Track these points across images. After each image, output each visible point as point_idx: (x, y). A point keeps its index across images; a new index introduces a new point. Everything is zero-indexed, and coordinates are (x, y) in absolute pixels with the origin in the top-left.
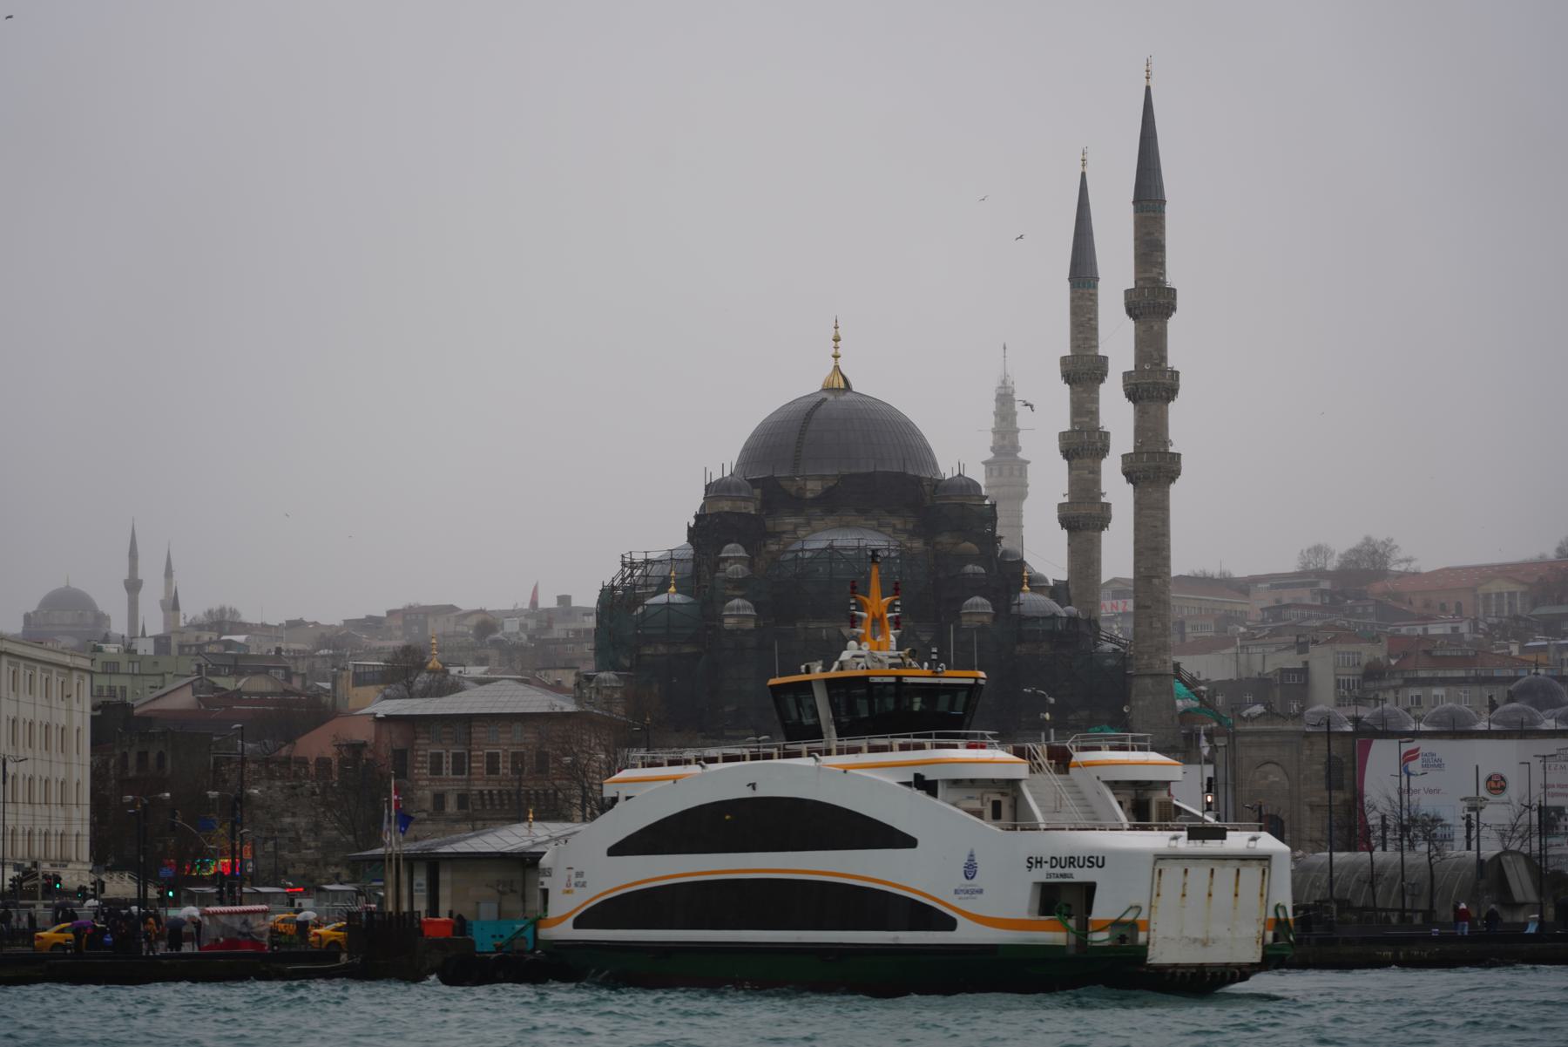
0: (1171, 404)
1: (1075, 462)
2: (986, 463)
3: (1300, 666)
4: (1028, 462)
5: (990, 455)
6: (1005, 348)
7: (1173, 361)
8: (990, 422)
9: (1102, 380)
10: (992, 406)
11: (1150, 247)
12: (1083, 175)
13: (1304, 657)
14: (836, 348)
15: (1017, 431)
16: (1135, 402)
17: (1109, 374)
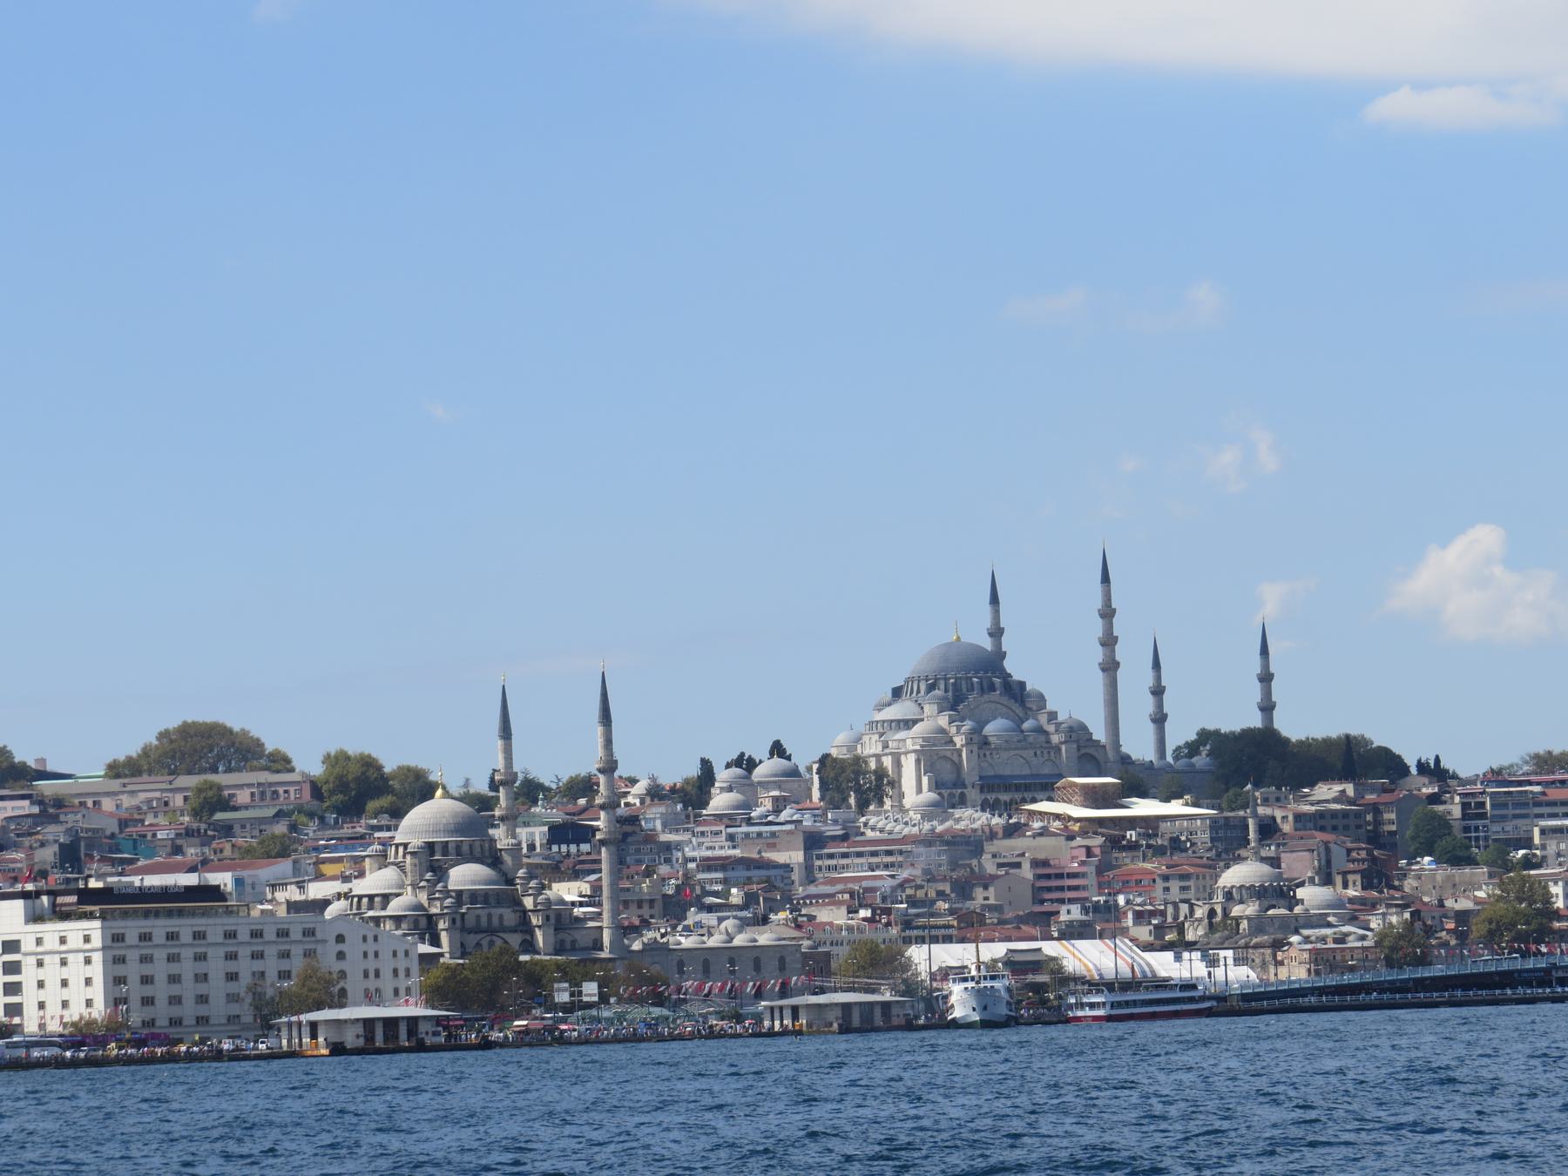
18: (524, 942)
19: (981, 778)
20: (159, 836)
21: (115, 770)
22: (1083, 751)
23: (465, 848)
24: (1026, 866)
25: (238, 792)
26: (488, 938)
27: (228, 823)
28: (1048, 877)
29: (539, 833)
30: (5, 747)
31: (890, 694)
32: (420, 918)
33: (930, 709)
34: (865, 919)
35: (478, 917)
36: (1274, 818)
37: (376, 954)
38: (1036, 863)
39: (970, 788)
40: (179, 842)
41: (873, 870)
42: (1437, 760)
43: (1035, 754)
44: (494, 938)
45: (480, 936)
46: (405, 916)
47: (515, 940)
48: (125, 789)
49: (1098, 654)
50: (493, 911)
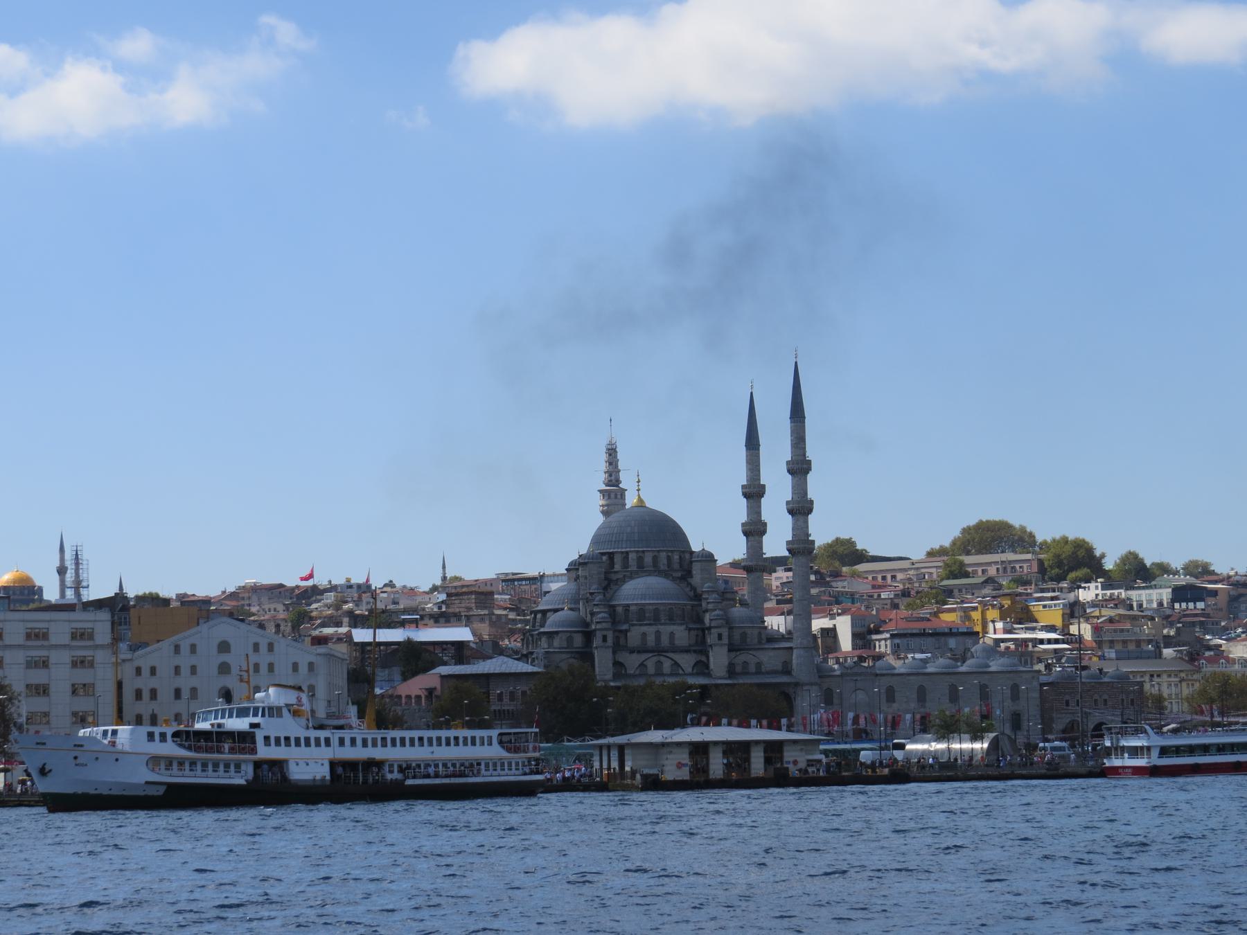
1: (751, 538)
3: (831, 626)
4: (626, 490)
5: (604, 487)
6: (611, 420)
7: (810, 495)
8: (603, 466)
9: (763, 497)
10: (604, 457)
11: (799, 440)
12: (752, 393)
13: (833, 622)
14: (638, 486)
15: (619, 471)
16: (793, 516)
17: (766, 493)
20: (882, 597)
21: (931, 554)
23: (648, 559)
25: (989, 568)
26: (655, 659)
27: (951, 588)
29: (1166, 594)
30: (851, 538)
32: (575, 635)
35: (644, 634)
37: (271, 667)
40: (896, 601)
44: (662, 659)
45: (643, 657)
46: (557, 633)
47: (687, 661)
48: (914, 566)
50: (661, 628)
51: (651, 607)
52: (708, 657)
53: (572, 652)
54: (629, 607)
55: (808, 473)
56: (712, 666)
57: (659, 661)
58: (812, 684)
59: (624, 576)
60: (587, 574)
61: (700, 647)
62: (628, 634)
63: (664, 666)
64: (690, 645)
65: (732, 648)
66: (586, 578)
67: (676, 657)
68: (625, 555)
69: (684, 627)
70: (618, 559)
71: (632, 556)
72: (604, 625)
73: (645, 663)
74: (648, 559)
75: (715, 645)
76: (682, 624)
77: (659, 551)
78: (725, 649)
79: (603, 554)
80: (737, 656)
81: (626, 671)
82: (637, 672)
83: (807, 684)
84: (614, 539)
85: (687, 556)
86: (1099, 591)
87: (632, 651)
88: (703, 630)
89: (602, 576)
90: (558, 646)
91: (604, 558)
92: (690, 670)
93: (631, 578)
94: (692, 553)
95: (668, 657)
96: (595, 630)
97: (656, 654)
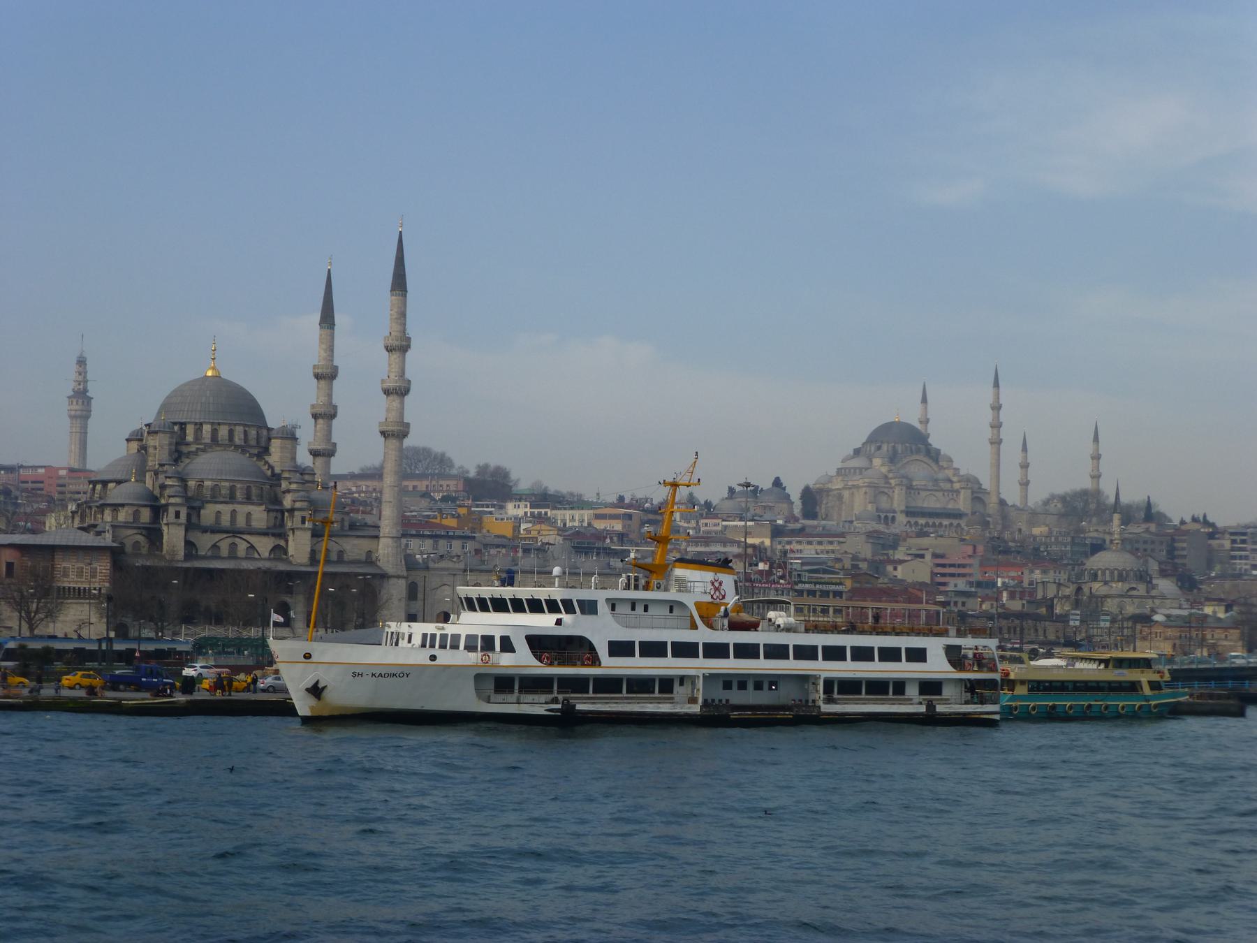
0: (406, 397)
2: (69, 397)
4: (92, 398)
8: (73, 375)
10: (75, 367)
18: (276, 548)
19: (907, 507)
22: (975, 495)
23: (223, 432)
24: (928, 557)
26: (230, 540)
28: (943, 566)
31: (852, 453)
33: (877, 462)
34: (761, 572)
36: (1104, 541)
38: (935, 556)
39: (899, 514)
41: (818, 554)
42: (1205, 516)
43: (944, 494)
44: (237, 539)
45: (218, 537)
46: (123, 505)
47: (264, 545)
49: (989, 433)
50: (238, 507)
51: (227, 484)
52: (287, 541)
53: (139, 528)
54: (203, 482)
55: (407, 351)
56: (291, 551)
57: (233, 543)
58: (398, 577)
59: (197, 449)
60: (157, 444)
61: (278, 531)
62: (202, 512)
63: (239, 548)
64: (268, 528)
65: (316, 534)
66: (155, 448)
67: (252, 539)
68: (198, 426)
69: (263, 507)
70: (190, 430)
71: (207, 428)
72: (177, 500)
73: (217, 544)
74: (223, 432)
75: (298, 529)
76: (261, 504)
77: (235, 425)
78: (309, 534)
79: (175, 424)
80: (318, 542)
81: (197, 552)
82: (209, 554)
83: (394, 577)
84: (186, 409)
85: (265, 432)
86: (528, 510)
87: (205, 530)
88: (282, 513)
89: (173, 448)
90: (124, 520)
91: (176, 428)
92: (266, 555)
93: (204, 450)
94: (269, 430)
95: (244, 539)
96: (167, 505)
97: (231, 535)
